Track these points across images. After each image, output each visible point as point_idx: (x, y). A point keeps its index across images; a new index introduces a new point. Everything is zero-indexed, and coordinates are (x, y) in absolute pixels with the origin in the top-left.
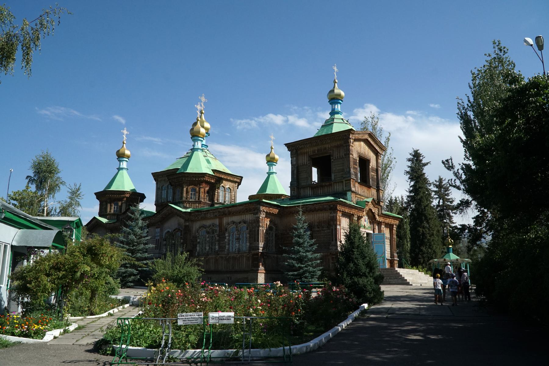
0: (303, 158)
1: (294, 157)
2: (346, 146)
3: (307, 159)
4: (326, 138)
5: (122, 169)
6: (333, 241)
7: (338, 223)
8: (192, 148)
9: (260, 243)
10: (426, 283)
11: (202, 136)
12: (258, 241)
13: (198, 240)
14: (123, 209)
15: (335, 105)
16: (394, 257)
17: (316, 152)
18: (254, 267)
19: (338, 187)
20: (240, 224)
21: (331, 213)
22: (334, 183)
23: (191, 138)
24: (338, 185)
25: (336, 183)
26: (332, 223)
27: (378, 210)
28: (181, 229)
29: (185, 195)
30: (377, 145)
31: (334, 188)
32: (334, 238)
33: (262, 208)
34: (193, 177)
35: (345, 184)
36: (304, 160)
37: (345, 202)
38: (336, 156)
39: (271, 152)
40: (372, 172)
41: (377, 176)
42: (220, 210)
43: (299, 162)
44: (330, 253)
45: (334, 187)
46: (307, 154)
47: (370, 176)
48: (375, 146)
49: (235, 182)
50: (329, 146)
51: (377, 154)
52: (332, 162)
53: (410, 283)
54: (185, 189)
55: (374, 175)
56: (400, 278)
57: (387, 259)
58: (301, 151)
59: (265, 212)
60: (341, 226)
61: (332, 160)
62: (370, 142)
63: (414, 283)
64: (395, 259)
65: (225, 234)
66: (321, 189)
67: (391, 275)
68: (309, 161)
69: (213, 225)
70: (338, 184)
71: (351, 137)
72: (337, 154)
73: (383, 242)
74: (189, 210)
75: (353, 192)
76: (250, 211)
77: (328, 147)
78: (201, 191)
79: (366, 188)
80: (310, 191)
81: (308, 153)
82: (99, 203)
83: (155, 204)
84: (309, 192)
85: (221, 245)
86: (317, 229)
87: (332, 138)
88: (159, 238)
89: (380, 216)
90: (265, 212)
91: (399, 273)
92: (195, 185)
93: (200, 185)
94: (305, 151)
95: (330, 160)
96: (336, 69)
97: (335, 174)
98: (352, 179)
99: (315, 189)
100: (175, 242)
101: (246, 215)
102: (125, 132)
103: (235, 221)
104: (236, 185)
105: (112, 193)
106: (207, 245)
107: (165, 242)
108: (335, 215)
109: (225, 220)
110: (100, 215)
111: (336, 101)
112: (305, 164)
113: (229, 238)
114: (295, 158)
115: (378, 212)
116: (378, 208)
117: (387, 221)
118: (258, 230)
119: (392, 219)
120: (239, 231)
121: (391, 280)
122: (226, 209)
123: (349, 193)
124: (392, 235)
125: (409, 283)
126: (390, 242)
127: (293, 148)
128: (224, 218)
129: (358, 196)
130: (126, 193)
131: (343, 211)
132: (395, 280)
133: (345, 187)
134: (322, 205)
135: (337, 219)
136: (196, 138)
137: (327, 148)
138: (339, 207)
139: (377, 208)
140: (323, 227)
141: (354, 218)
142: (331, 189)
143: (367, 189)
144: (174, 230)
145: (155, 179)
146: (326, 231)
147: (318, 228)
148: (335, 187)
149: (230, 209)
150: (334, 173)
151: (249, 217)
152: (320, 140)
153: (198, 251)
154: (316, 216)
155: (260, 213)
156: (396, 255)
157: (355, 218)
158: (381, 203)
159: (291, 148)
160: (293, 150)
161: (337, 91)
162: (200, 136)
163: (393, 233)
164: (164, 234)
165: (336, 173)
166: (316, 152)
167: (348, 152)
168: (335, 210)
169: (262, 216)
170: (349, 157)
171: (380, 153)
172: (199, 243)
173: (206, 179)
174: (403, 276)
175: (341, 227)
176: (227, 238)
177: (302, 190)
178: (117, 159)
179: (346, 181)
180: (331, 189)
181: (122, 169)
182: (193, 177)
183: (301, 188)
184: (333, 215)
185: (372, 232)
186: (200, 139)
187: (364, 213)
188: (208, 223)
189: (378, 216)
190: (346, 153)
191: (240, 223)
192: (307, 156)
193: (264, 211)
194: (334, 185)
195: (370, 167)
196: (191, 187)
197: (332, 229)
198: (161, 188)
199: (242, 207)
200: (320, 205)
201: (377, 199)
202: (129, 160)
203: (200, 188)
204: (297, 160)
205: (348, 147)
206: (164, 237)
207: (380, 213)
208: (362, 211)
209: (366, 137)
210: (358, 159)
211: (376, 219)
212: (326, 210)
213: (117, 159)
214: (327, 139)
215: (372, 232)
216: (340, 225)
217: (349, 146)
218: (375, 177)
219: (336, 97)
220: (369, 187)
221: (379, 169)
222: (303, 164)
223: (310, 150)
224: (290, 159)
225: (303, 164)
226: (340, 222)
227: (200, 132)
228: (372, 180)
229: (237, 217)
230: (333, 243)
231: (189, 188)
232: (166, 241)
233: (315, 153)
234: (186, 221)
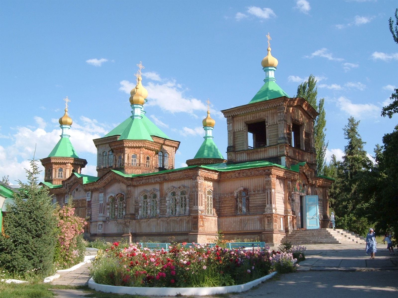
1: (230, 123)
6: (268, 204)
7: (273, 187)
9: (199, 206)
12: (197, 205)
13: (140, 204)
18: (194, 229)
20: (180, 189)
21: (266, 178)
23: (131, 105)
28: (123, 194)
29: (126, 161)
36: (240, 126)
39: (208, 116)
42: (161, 176)
49: (173, 147)
56: (330, 238)
60: (276, 190)
61: (267, 126)
65: (165, 199)
66: (256, 154)
69: (154, 190)
74: (131, 176)
76: (189, 177)
80: (246, 156)
83: (97, 170)
84: (244, 157)
85: (162, 209)
86: (253, 193)
88: (102, 202)
91: (329, 233)
95: (265, 126)
96: (269, 37)
100: (118, 206)
101: (186, 180)
102: (67, 100)
103: (175, 186)
104: (174, 150)
106: (148, 209)
107: (108, 206)
109: (166, 186)
110: (46, 181)
112: (241, 130)
113: (169, 203)
114: (231, 125)
118: (197, 195)
122: (166, 175)
125: (338, 242)
128: (165, 183)
134: (258, 170)
144: (117, 195)
145: (96, 146)
147: (254, 191)
149: (170, 174)
151: (187, 183)
153: (140, 214)
160: (229, 116)
164: (107, 199)
169: (201, 181)
172: (141, 207)
173: (147, 145)
174: (333, 236)
175: (276, 191)
176: (168, 202)
178: (60, 126)
184: (268, 180)
188: (149, 188)
191: (179, 188)
192: (243, 122)
197: (267, 193)
198: (102, 154)
200: (255, 170)
202: (71, 127)
204: (233, 126)
206: (107, 201)
213: (60, 126)
216: (275, 189)
224: (227, 125)
225: (239, 130)
227: (139, 100)
229: (177, 182)
230: (268, 206)
232: (109, 205)
234: (128, 186)
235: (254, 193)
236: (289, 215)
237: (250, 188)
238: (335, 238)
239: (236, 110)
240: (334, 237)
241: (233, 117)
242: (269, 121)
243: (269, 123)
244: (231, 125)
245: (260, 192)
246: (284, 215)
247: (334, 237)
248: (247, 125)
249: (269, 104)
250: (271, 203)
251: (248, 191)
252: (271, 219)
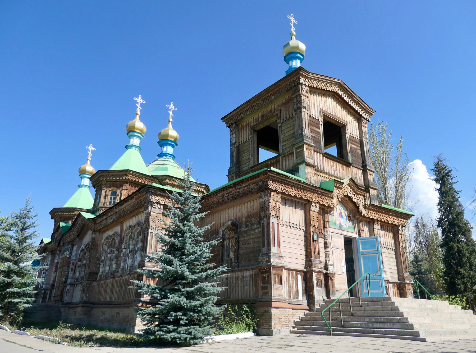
0: (245, 132)
1: (233, 134)
2: (296, 97)
3: (249, 132)
4: (269, 95)
5: (82, 186)
6: (264, 246)
7: (273, 213)
10: (465, 332)
11: (139, 132)
15: (292, 62)
16: (404, 279)
17: (260, 119)
19: (287, 163)
21: (260, 197)
22: (282, 157)
24: (287, 160)
25: (285, 156)
26: (263, 214)
27: (365, 199)
30: (357, 104)
31: (282, 165)
32: (266, 241)
33: (153, 198)
34: (113, 175)
35: (296, 155)
37: (287, 177)
40: (351, 143)
41: (361, 150)
43: (241, 138)
44: (260, 270)
45: (283, 163)
46: (250, 126)
47: (349, 150)
48: (353, 104)
50: (276, 106)
51: (358, 118)
52: (280, 127)
53: (422, 336)
54: (103, 192)
55: (356, 149)
56: (398, 322)
57: (387, 282)
58: (243, 123)
59: (161, 205)
60: (281, 219)
62: (343, 99)
63: (433, 333)
64: (406, 281)
67: (380, 313)
68: (251, 134)
71: (302, 80)
73: (377, 252)
75: (308, 165)
78: (123, 194)
79: (340, 165)
81: (251, 123)
82: (54, 223)
87: (277, 91)
89: (369, 209)
90: (161, 205)
91: (397, 309)
92: (117, 187)
93: (122, 186)
94: (247, 122)
96: (292, 19)
97: (284, 144)
98: (307, 144)
100: (86, 263)
105: (61, 211)
108: (266, 198)
111: (293, 55)
113: (126, 252)
114: (234, 135)
115: (365, 201)
116: (364, 196)
117: (385, 218)
119: (393, 216)
120: (133, 239)
121: (378, 325)
123: (302, 167)
124: (398, 243)
125: (417, 334)
126: (396, 255)
129: (324, 175)
130: (76, 210)
131: (283, 193)
132: (386, 326)
133: (296, 158)
135: (269, 206)
136: (131, 133)
137: (273, 110)
138: (271, 185)
139: (361, 195)
140: (253, 224)
141: (312, 208)
143: (342, 167)
146: (257, 231)
152: (262, 100)
153: (100, 273)
154: (243, 207)
155: (151, 205)
156: (407, 274)
157: (315, 209)
158: (371, 190)
159: (229, 122)
161: (294, 42)
162: (136, 131)
163: (399, 239)
165: (284, 142)
166: (260, 119)
167: (299, 105)
168: (266, 190)
170: (301, 112)
171: (364, 117)
173: (130, 177)
174: (405, 316)
175: (281, 222)
176: (124, 250)
179: (297, 148)
181: (82, 186)
182: (113, 175)
185: (357, 236)
186: (136, 134)
187: (335, 201)
189: (365, 208)
190: (296, 107)
193: (158, 203)
194: (282, 160)
195: (347, 135)
196: (110, 189)
199: (132, 202)
201: (364, 185)
203: (122, 190)
204: (238, 137)
205: (298, 97)
207: (368, 203)
208: (328, 197)
209: (335, 89)
210: (321, 119)
211: (360, 213)
212: (253, 193)
214: (271, 94)
215: (357, 236)
216: (278, 218)
217: (300, 95)
218: (359, 151)
219: (292, 50)
220: (348, 165)
221: (364, 139)
223: (252, 120)
224: (229, 137)
225: (245, 141)
226: (277, 210)
228: (352, 155)
230: (264, 250)
231: (108, 191)
233: (258, 121)
235: (246, 229)
236: (314, 269)
237: (241, 221)
238: (410, 321)
239: (239, 112)
240: (407, 319)
241: (237, 123)
242: (282, 116)
244: (234, 135)
245: (255, 226)
246: (305, 270)
247: (407, 319)
248: (256, 133)
249: (280, 89)
251: (237, 225)
252: (268, 276)
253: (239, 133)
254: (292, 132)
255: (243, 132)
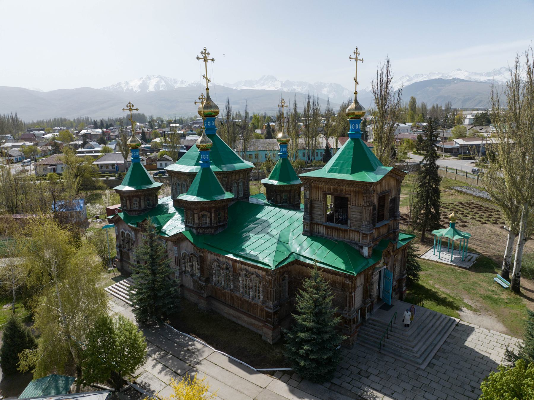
0: (317, 192)
6: (346, 306)
8: (202, 60)
14: (142, 204)
31: (349, 235)
38: (354, 203)
61: (349, 206)
66: (335, 232)
70: (354, 233)
72: (355, 201)
77: (346, 190)
80: (324, 229)
97: (352, 221)
99: (329, 230)
114: (308, 192)
127: (306, 181)
137: (344, 190)
140: (337, 288)
142: (346, 235)
146: (340, 292)
148: (351, 235)
150: (351, 220)
166: (332, 190)
176: (241, 282)
177: (315, 226)
180: (346, 235)
183: (314, 224)
197: (347, 295)
204: (311, 193)
206: (182, 256)
222: (317, 199)
242: (352, 201)
243: (352, 203)
250: (350, 306)
253: (311, 190)
254: (359, 216)
255: (315, 191)
